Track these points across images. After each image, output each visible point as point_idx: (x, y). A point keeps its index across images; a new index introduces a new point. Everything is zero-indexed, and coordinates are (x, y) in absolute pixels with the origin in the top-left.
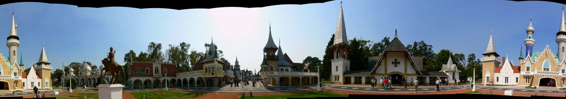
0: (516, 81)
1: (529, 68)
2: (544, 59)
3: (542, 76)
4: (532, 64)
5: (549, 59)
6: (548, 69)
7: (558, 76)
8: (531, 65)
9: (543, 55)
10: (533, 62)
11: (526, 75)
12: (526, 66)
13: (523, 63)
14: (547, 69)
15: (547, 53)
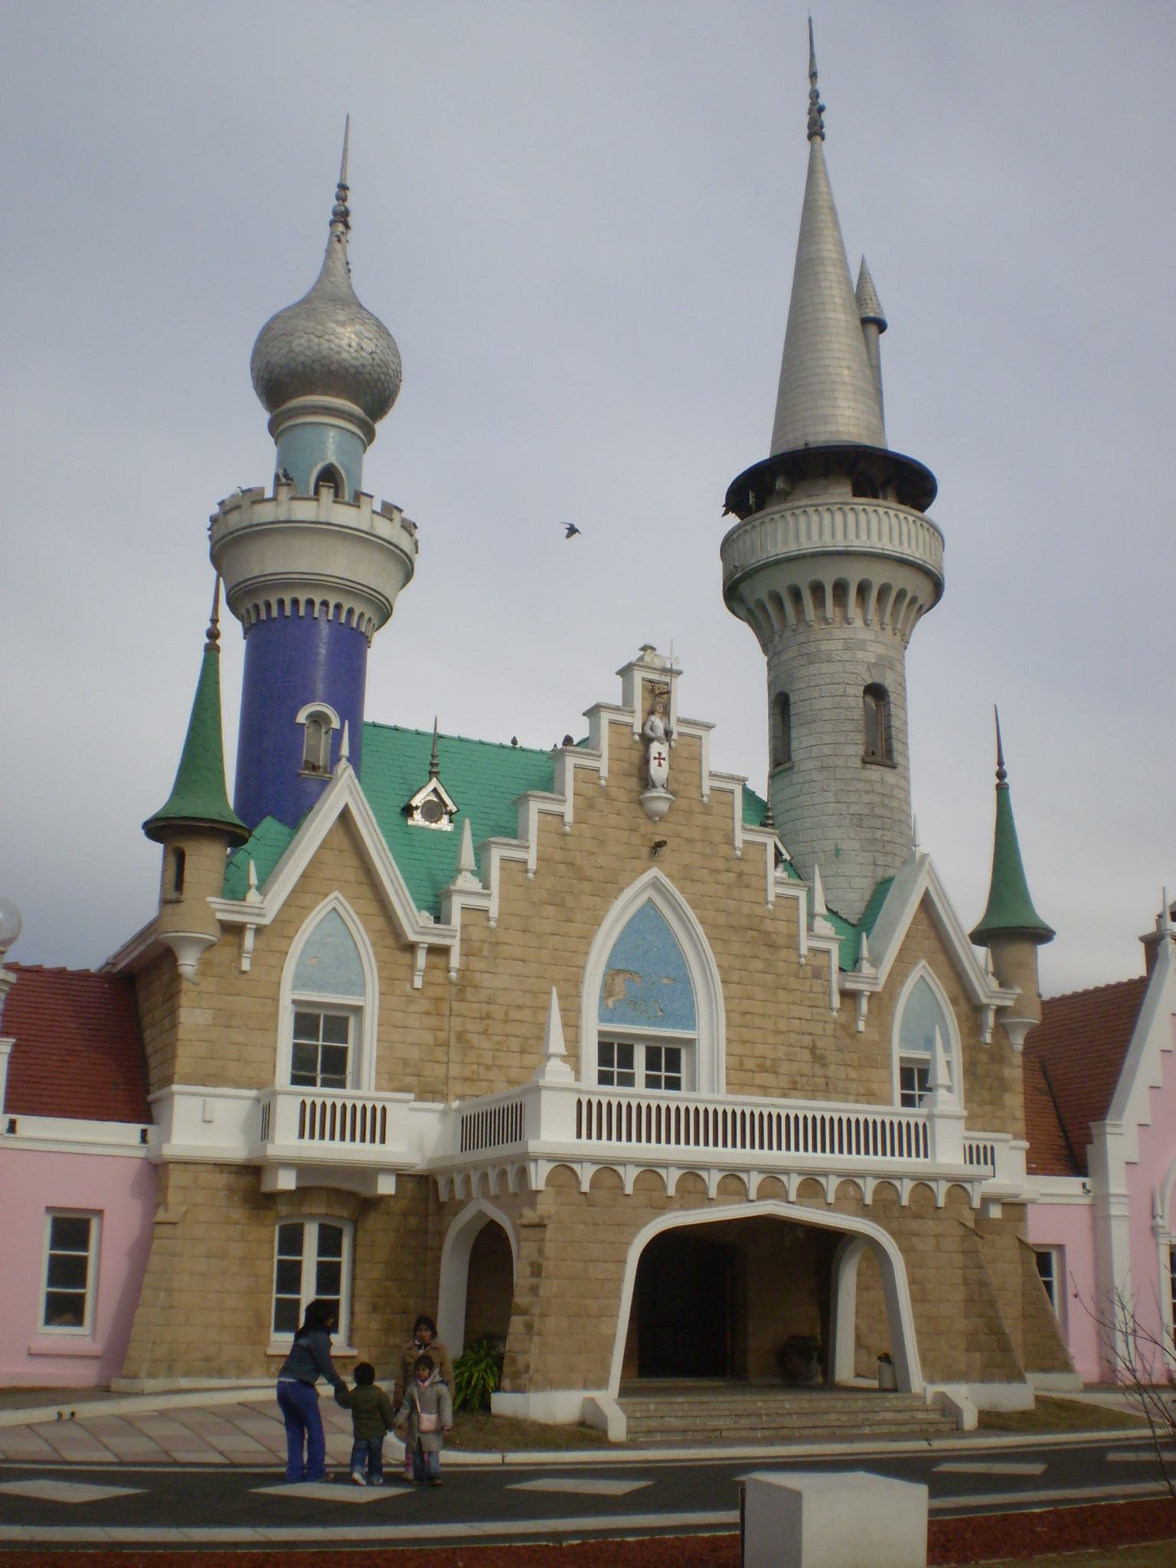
0: (41, 1289)
1: (338, 1023)
2: (610, 887)
3: (672, 1177)
4: (411, 948)
5: (685, 876)
6: (674, 1063)
7: (923, 1184)
8: (387, 980)
9: (586, 804)
10: (415, 923)
11: (303, 1168)
12: (287, 996)
13: (233, 930)
14: (652, 1063)
15: (659, 772)
